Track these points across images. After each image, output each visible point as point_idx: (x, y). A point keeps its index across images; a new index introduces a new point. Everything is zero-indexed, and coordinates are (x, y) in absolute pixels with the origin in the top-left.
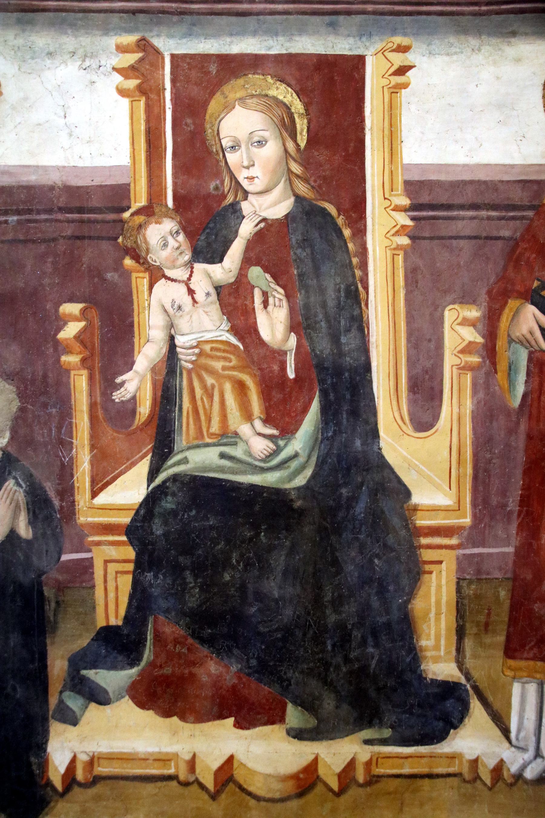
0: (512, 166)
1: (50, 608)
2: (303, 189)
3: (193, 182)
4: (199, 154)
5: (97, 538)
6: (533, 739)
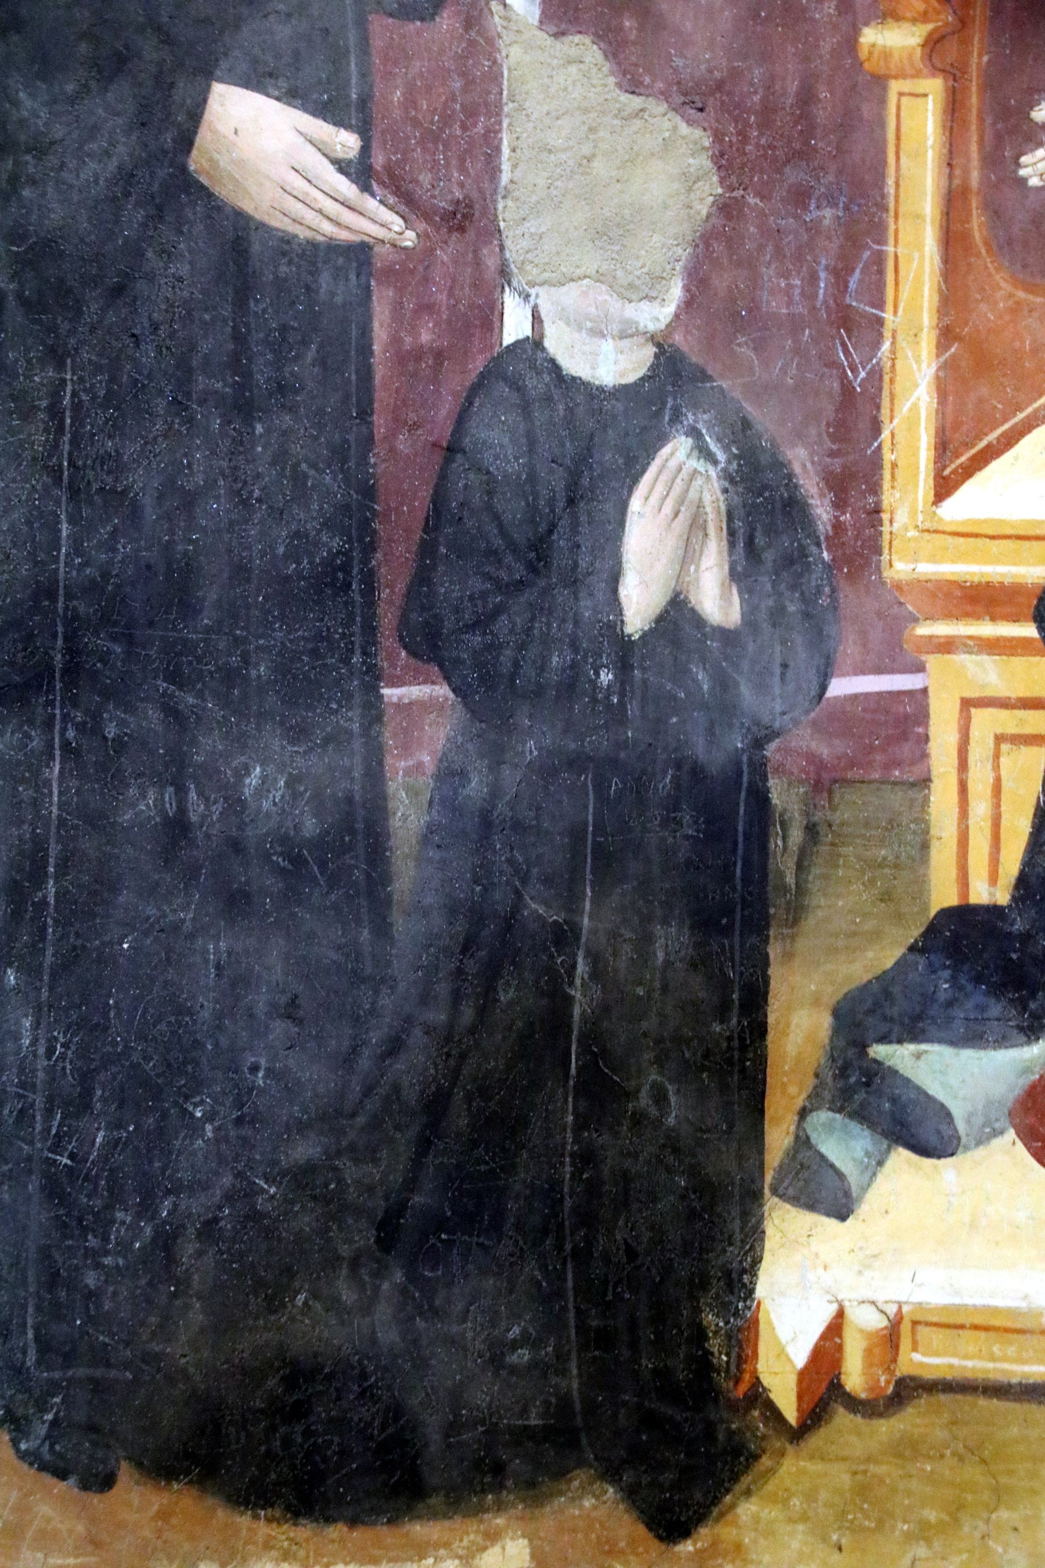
1: (785, 847)
5: (942, 629)
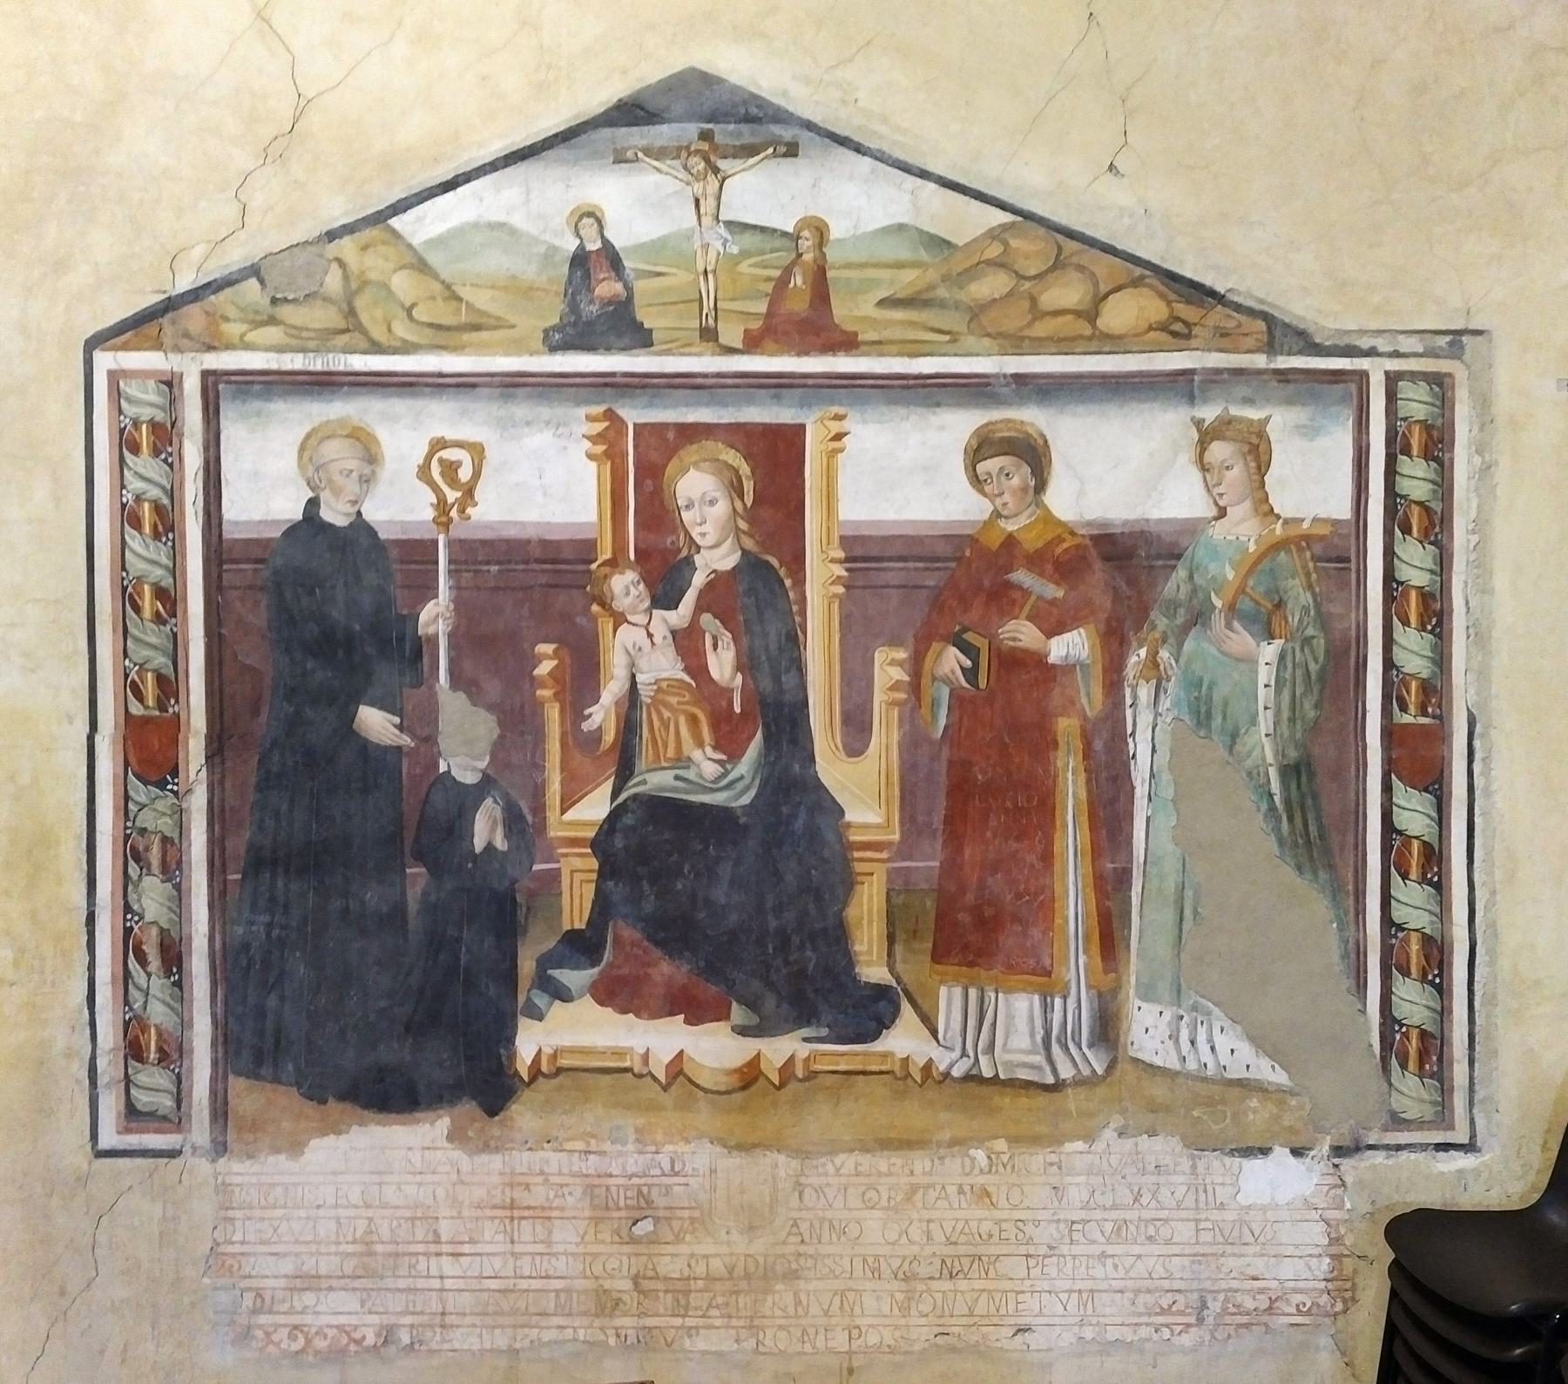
0: (936, 522)
1: (521, 913)
2: (749, 544)
3: (652, 537)
4: (658, 512)
6: (960, 1039)
